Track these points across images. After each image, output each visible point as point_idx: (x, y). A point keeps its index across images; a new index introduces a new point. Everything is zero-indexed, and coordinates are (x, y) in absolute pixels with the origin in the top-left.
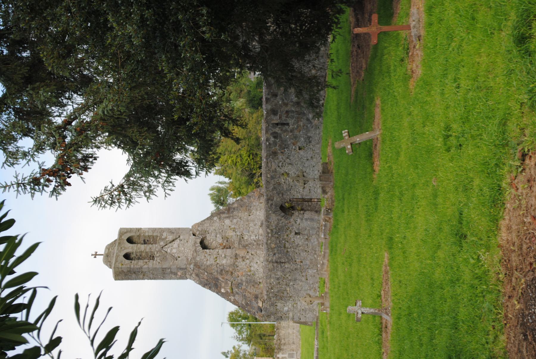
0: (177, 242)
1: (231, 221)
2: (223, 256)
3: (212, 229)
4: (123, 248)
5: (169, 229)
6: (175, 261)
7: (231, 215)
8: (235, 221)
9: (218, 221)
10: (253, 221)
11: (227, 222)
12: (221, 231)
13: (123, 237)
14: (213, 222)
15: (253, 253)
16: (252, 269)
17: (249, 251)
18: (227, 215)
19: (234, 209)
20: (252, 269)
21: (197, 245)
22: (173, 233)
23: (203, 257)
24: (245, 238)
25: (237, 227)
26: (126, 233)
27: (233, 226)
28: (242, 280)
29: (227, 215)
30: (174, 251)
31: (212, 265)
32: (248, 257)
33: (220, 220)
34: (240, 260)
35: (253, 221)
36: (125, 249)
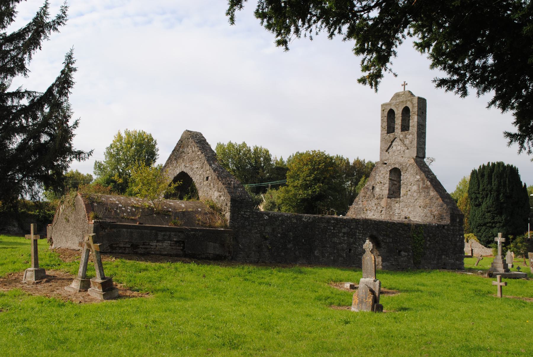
2: (383, 188)
8: (415, 194)
9: (416, 179)
11: (415, 188)
13: (408, 102)
16: (369, 212)
17: (384, 209)
18: (421, 187)
19: (428, 192)
20: (369, 212)
24: (396, 205)
25: (408, 196)
27: (409, 193)
28: (359, 204)
29: (421, 187)
30: (394, 148)
31: (376, 180)
32: (379, 208)
34: (376, 201)
36: (397, 108)
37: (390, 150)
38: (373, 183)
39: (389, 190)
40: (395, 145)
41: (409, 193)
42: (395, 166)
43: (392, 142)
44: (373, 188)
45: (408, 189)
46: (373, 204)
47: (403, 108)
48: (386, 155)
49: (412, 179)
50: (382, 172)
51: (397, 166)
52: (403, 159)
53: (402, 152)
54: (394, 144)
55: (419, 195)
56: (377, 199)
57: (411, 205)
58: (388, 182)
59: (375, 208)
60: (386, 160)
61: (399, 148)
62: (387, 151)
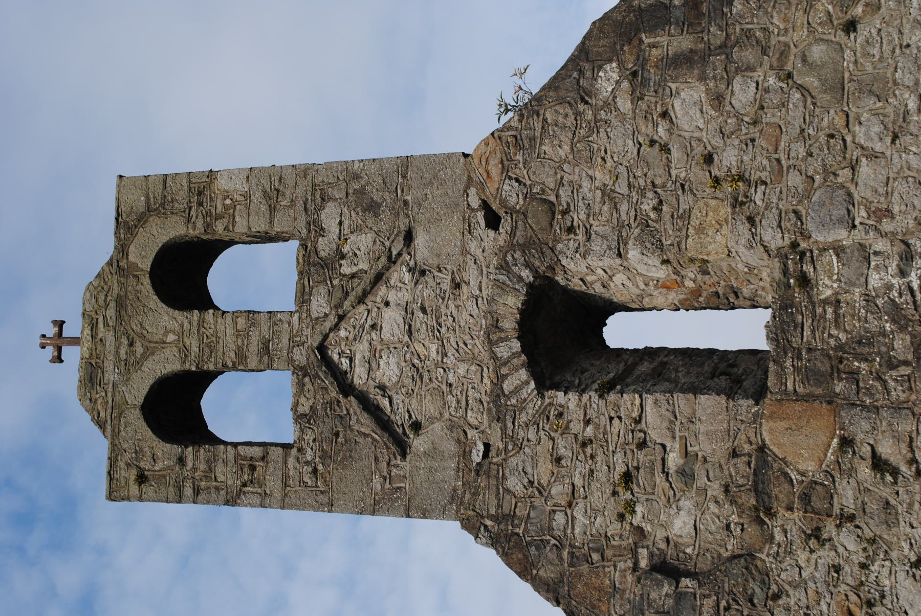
0: (400, 287)
1: (718, 100)
2: (674, 460)
3: (590, 181)
4: (139, 349)
5: (349, 173)
6: (405, 466)
7: (716, 35)
8: (742, 94)
9: (625, 104)
10: (880, 88)
11: (688, 101)
12: (647, 206)
14: (596, 126)
15: (886, 449)
17: (860, 428)
18: (683, 42)
21: (503, 351)
22: (373, 208)
23: (543, 471)
24: (826, 289)
25: (758, 164)
26: (142, 219)
27: (729, 158)
29: (683, 42)
30: (389, 369)
33: (637, 98)
34: (789, 523)
35: (880, 88)
37: (400, 410)
38: (619, 573)
39: (695, 390)
40: (371, 364)
41: (729, 158)
42: (509, 324)
43: (346, 388)
44: (667, 568)
45: (699, 175)
46: (812, 563)
47: (154, 301)
48: (433, 453)
49: (619, 142)
50: (543, 471)
51: (513, 302)
52: (472, 275)
53: (426, 292)
54: (359, 376)
55: (748, 55)
56: (763, 511)
57: (833, 118)
58: (629, 402)
59: (847, 540)
60: (466, 454)
61: (392, 320)
62: (403, 448)
